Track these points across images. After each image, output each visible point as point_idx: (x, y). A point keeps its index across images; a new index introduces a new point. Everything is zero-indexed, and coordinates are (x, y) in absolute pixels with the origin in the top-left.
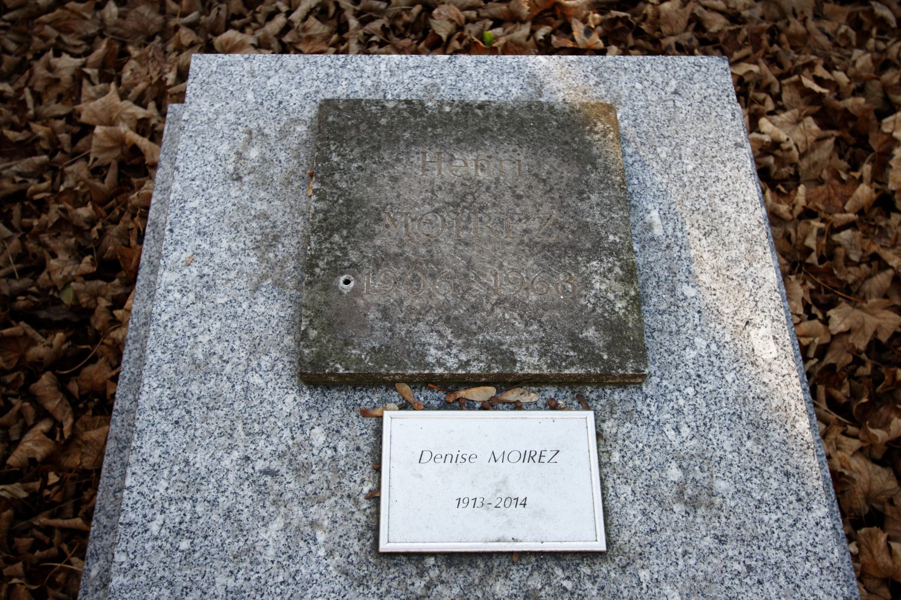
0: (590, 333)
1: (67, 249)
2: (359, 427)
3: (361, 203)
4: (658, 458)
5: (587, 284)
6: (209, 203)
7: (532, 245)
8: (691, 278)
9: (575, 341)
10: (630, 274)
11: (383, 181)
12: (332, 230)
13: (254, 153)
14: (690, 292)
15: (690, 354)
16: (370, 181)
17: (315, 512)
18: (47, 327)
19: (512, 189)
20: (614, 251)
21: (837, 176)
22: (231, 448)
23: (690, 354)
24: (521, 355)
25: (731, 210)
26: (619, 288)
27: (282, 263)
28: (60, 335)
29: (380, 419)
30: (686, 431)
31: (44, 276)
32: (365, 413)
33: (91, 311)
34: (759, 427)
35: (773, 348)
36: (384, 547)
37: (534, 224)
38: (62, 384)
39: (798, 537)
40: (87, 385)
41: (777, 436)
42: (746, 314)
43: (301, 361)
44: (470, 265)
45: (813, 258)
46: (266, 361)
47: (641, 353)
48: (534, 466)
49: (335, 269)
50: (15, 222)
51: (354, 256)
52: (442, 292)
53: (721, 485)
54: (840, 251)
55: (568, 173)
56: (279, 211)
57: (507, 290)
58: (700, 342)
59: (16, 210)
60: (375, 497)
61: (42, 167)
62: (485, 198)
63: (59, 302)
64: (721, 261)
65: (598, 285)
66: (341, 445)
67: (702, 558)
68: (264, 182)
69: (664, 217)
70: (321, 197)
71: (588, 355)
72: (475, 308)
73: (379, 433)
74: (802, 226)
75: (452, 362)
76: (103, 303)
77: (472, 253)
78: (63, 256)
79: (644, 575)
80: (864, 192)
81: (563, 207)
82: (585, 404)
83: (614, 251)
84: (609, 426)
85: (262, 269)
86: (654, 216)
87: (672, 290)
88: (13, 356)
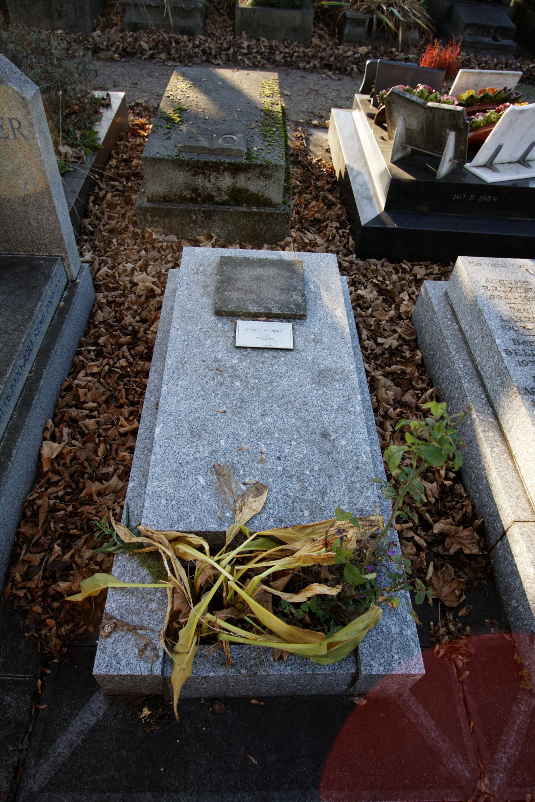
0: (292, 306)
1: (131, 314)
2: (231, 325)
3: (231, 278)
4: (308, 333)
5: (292, 296)
6: (189, 278)
7: (277, 288)
8: (320, 299)
9: (287, 307)
10: (303, 295)
11: (238, 273)
12: (224, 283)
13: (202, 269)
14: (320, 302)
15: (319, 314)
16: (234, 273)
17: (219, 339)
18: (125, 334)
19: (273, 277)
20: (300, 290)
21: (384, 309)
22: (197, 327)
23: (319, 314)
24: (273, 309)
25: (333, 286)
26: (300, 298)
27: (210, 292)
28: (129, 337)
29: (236, 323)
30: (316, 329)
31: (123, 321)
32: (232, 321)
33: (138, 332)
34: (336, 329)
35: (341, 314)
36: (237, 345)
37: (278, 284)
38: (129, 350)
39: (343, 349)
40: (136, 352)
41: (340, 331)
42: (335, 307)
43: (215, 307)
44: (260, 291)
45: (373, 328)
46: (206, 310)
47: (305, 310)
48: (276, 333)
49: (225, 290)
50: (113, 308)
51: (230, 288)
52: (253, 296)
53: (324, 339)
54: (381, 326)
55: (288, 274)
56: (209, 281)
57: (270, 297)
58: (322, 312)
59: (113, 305)
60: (234, 337)
61: (121, 294)
62: (265, 278)
63: (127, 329)
64: (329, 297)
65: (294, 297)
66: (226, 327)
67: (318, 352)
68: (205, 275)
69: (314, 287)
70: (221, 276)
71: (291, 310)
72: (261, 300)
73: (236, 325)
74: (370, 319)
75: (255, 310)
76: (142, 329)
77: (262, 289)
78: (129, 316)
79: (303, 354)
80: (392, 313)
81: (286, 281)
82: (289, 322)
83: (300, 290)
84: (296, 327)
85: (204, 292)
86: (312, 287)
87: (315, 302)
88: (115, 341)
